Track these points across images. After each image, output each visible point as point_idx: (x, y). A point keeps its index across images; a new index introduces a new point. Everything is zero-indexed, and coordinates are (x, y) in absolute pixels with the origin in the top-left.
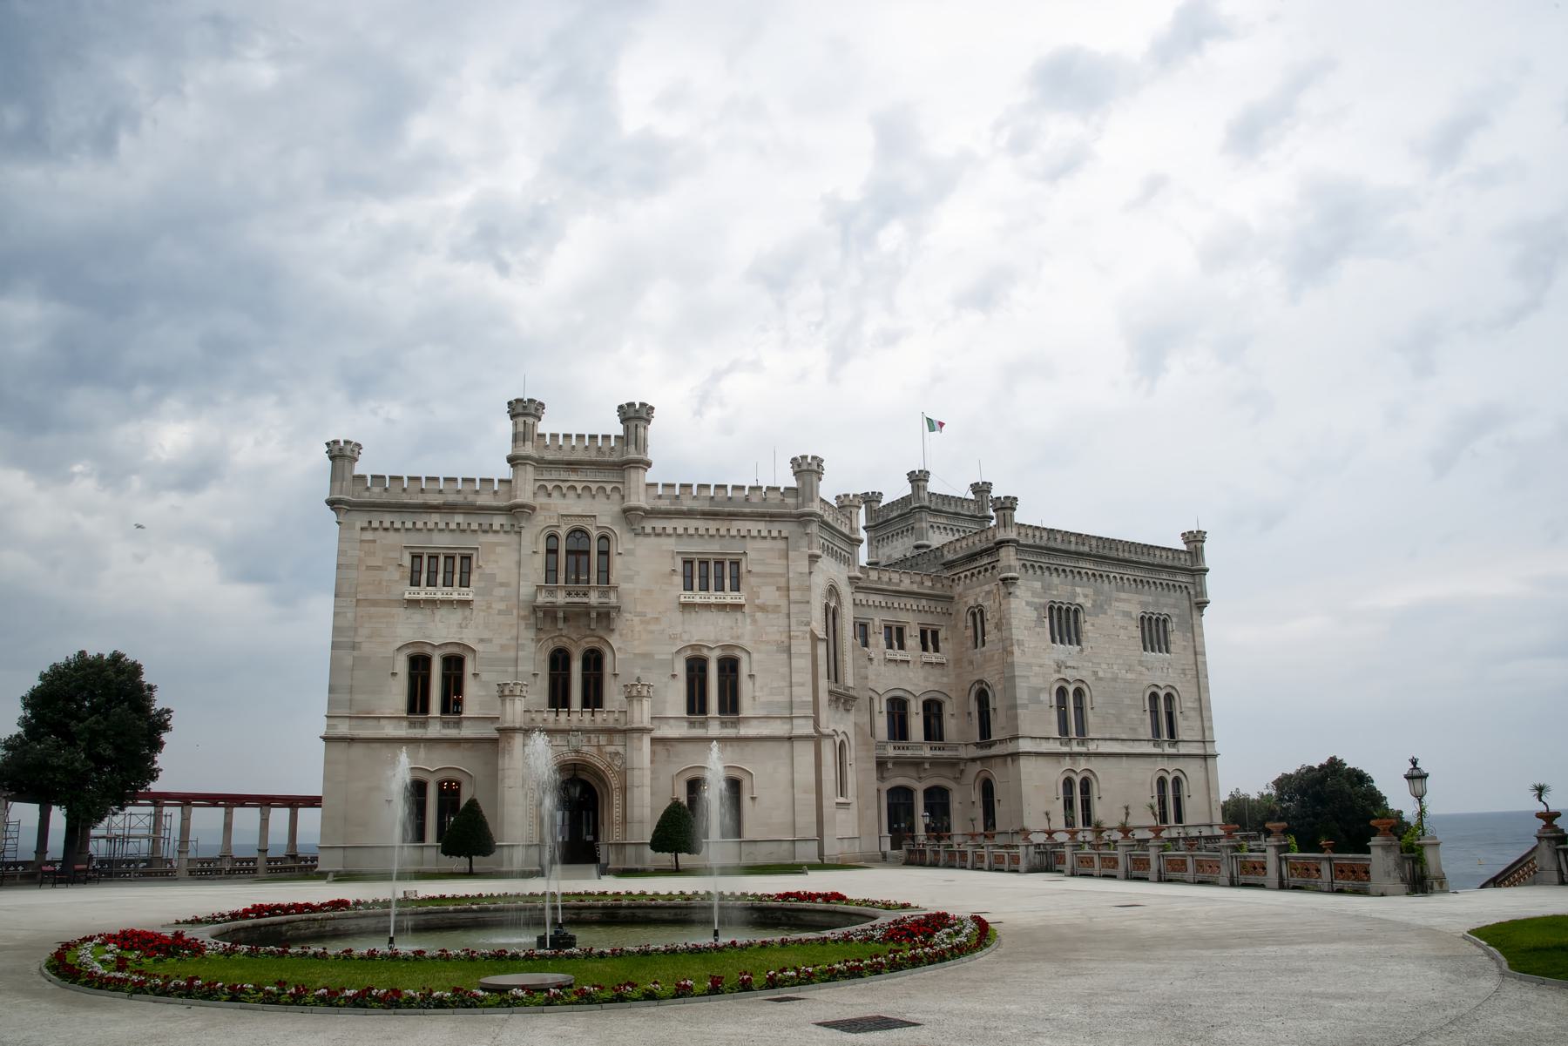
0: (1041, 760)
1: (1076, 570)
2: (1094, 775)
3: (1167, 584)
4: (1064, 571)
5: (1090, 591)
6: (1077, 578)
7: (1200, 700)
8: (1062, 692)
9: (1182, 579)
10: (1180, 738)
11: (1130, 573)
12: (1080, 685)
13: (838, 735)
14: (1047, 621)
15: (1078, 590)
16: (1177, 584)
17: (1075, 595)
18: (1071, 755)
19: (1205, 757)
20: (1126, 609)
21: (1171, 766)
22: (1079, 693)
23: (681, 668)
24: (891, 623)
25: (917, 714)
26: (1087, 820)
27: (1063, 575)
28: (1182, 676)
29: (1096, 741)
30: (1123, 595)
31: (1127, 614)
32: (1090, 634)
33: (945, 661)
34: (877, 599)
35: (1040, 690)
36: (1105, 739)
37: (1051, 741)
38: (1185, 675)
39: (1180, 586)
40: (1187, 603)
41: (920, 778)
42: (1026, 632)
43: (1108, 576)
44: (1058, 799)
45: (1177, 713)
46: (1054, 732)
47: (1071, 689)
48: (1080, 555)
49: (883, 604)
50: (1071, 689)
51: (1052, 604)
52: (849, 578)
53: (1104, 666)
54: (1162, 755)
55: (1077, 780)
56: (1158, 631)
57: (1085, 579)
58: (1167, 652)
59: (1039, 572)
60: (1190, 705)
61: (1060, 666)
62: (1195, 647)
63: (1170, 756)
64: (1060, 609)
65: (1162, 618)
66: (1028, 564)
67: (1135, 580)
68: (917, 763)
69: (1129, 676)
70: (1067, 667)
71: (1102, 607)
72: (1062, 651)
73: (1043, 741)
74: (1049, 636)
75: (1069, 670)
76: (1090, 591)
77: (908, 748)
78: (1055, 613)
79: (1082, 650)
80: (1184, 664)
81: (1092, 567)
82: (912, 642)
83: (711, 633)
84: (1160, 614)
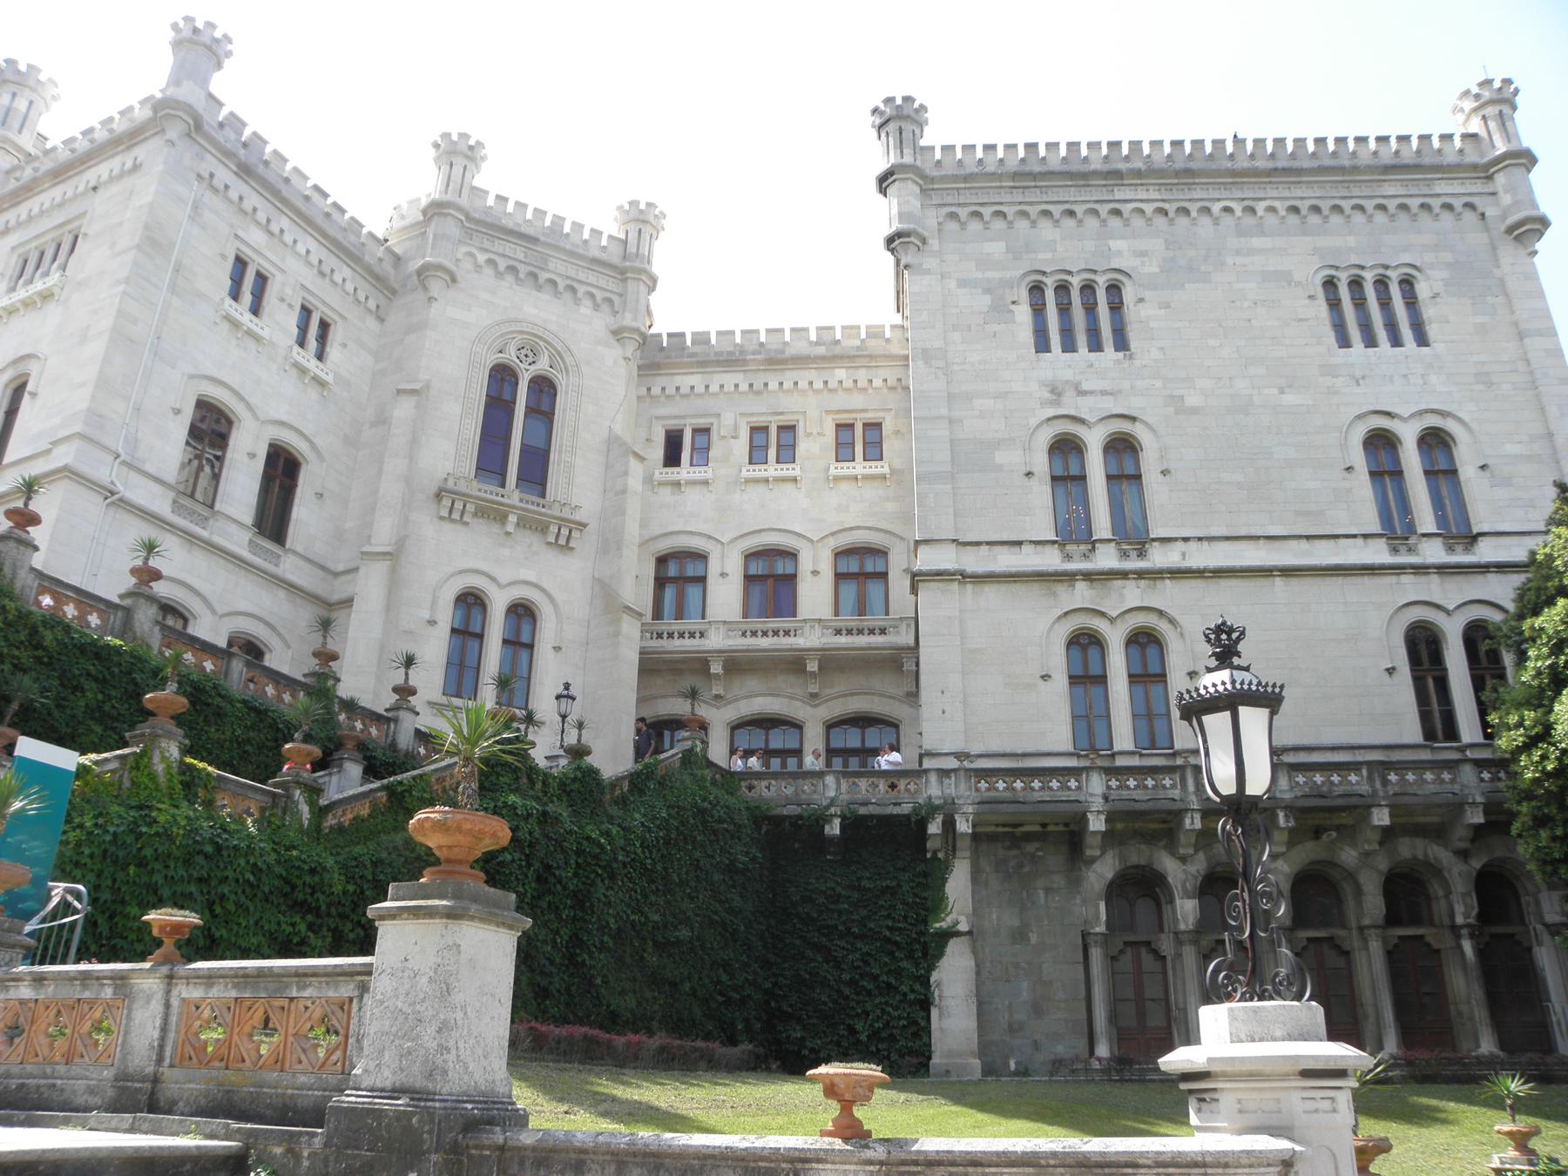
1: (1104, 209)
2: (1172, 621)
3: (1403, 207)
4: (1071, 213)
5: (1155, 245)
6: (1115, 222)
8: (1066, 448)
10: (1486, 529)
11: (1278, 195)
12: (1125, 426)
13: (500, 586)
14: (1024, 313)
15: (1116, 245)
16: (1436, 203)
18: (1088, 576)
20: (1271, 268)
21: (1451, 592)
22: (1122, 447)
24: (770, 418)
25: (815, 573)
27: (1069, 223)
28: (1481, 387)
29: (1180, 544)
30: (1257, 242)
31: (1284, 278)
32: (1152, 324)
33: (886, 470)
34: (730, 379)
36: (1211, 539)
37: (1026, 548)
38: (1490, 384)
39: (1448, 207)
40: (1476, 238)
41: (814, 696)
42: (957, 336)
43: (1206, 210)
44: (1046, 677)
45: (1468, 472)
47: (1094, 441)
48: (1116, 175)
49: (744, 387)
50: (1094, 441)
51: (1039, 277)
52: (615, 333)
54: (1420, 569)
55: (1115, 639)
56: (1385, 303)
57: (1138, 222)
58: (1422, 340)
59: (999, 224)
60: (1511, 449)
61: (1056, 392)
62: (1516, 324)
63: (1443, 569)
64: (1062, 288)
65: (1394, 275)
66: (963, 213)
67: (1295, 210)
68: (794, 664)
69: (1289, 399)
70: (1082, 393)
73: (1005, 549)
74: (1026, 334)
75: (1089, 401)
76: (1155, 245)
77: (765, 634)
78: (1050, 295)
79: (1131, 357)
80: (1484, 363)
81: (1156, 196)
82: (815, 445)
84: (1387, 267)
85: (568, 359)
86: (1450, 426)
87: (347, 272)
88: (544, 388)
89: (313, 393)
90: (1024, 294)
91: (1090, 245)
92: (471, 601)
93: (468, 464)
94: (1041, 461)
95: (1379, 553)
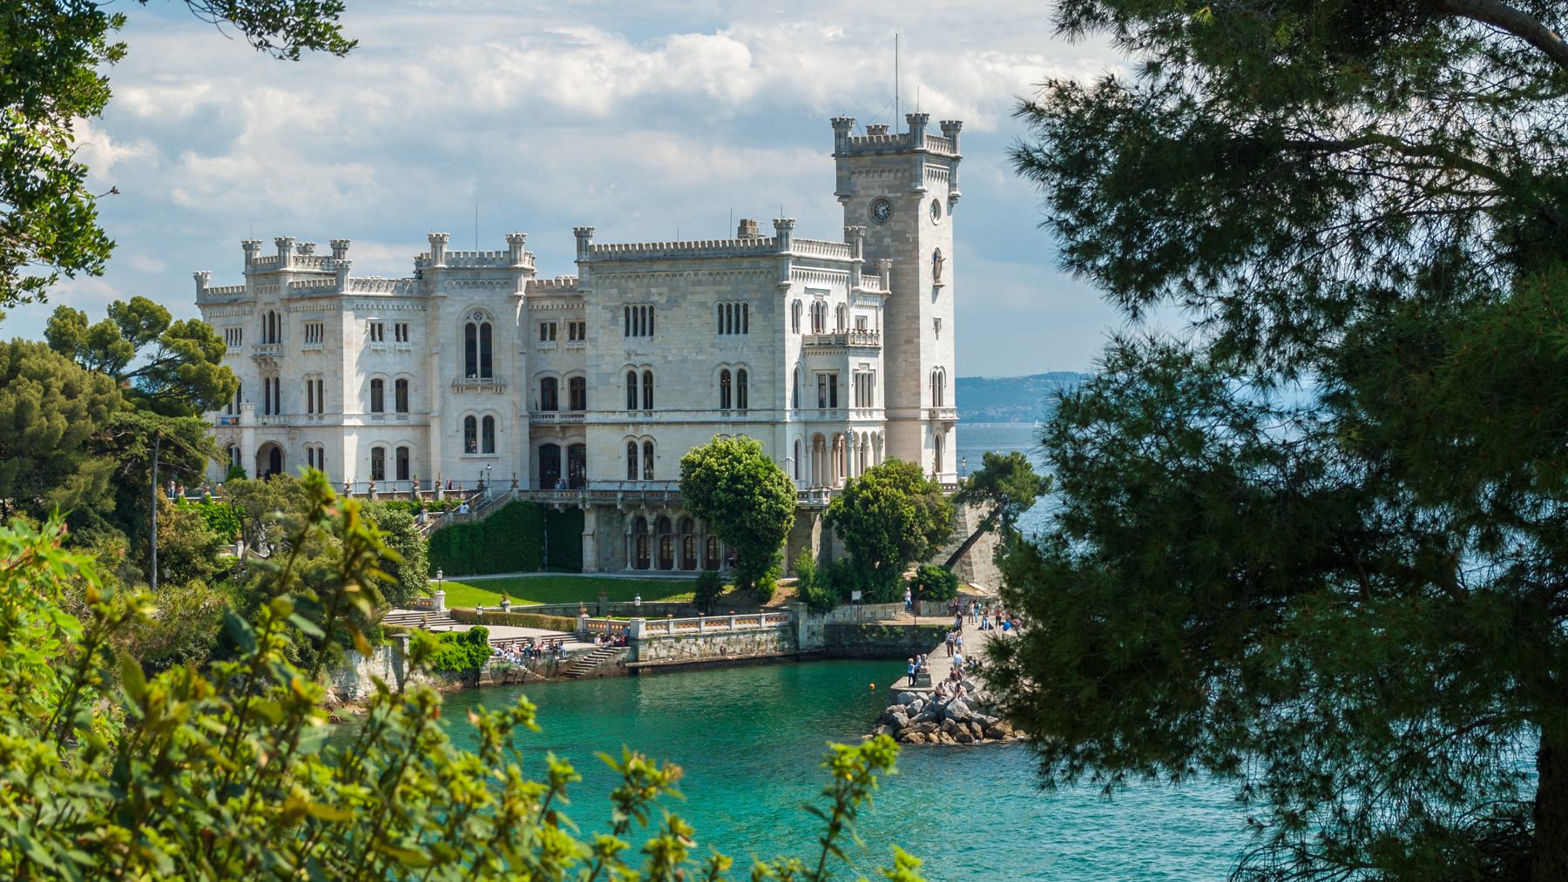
0: (606, 427)
5: (665, 290)
7: (773, 373)
8: (632, 377)
9: (764, 263)
14: (622, 320)
15: (653, 290)
17: (649, 294)
19: (773, 423)
22: (648, 377)
23: (304, 387)
30: (699, 289)
31: (703, 305)
34: (560, 302)
35: (610, 375)
46: (623, 405)
53: (674, 351)
54: (726, 423)
60: (763, 378)
63: (734, 423)
64: (635, 309)
67: (711, 274)
69: (699, 357)
71: (676, 301)
72: (633, 342)
74: (622, 330)
76: (665, 290)
83: (313, 364)
85: (494, 315)
86: (747, 369)
87: (408, 303)
88: (486, 329)
89: (406, 355)
90: (623, 312)
91: (644, 290)
92: (470, 422)
93: (463, 371)
94: (623, 381)
95: (718, 417)
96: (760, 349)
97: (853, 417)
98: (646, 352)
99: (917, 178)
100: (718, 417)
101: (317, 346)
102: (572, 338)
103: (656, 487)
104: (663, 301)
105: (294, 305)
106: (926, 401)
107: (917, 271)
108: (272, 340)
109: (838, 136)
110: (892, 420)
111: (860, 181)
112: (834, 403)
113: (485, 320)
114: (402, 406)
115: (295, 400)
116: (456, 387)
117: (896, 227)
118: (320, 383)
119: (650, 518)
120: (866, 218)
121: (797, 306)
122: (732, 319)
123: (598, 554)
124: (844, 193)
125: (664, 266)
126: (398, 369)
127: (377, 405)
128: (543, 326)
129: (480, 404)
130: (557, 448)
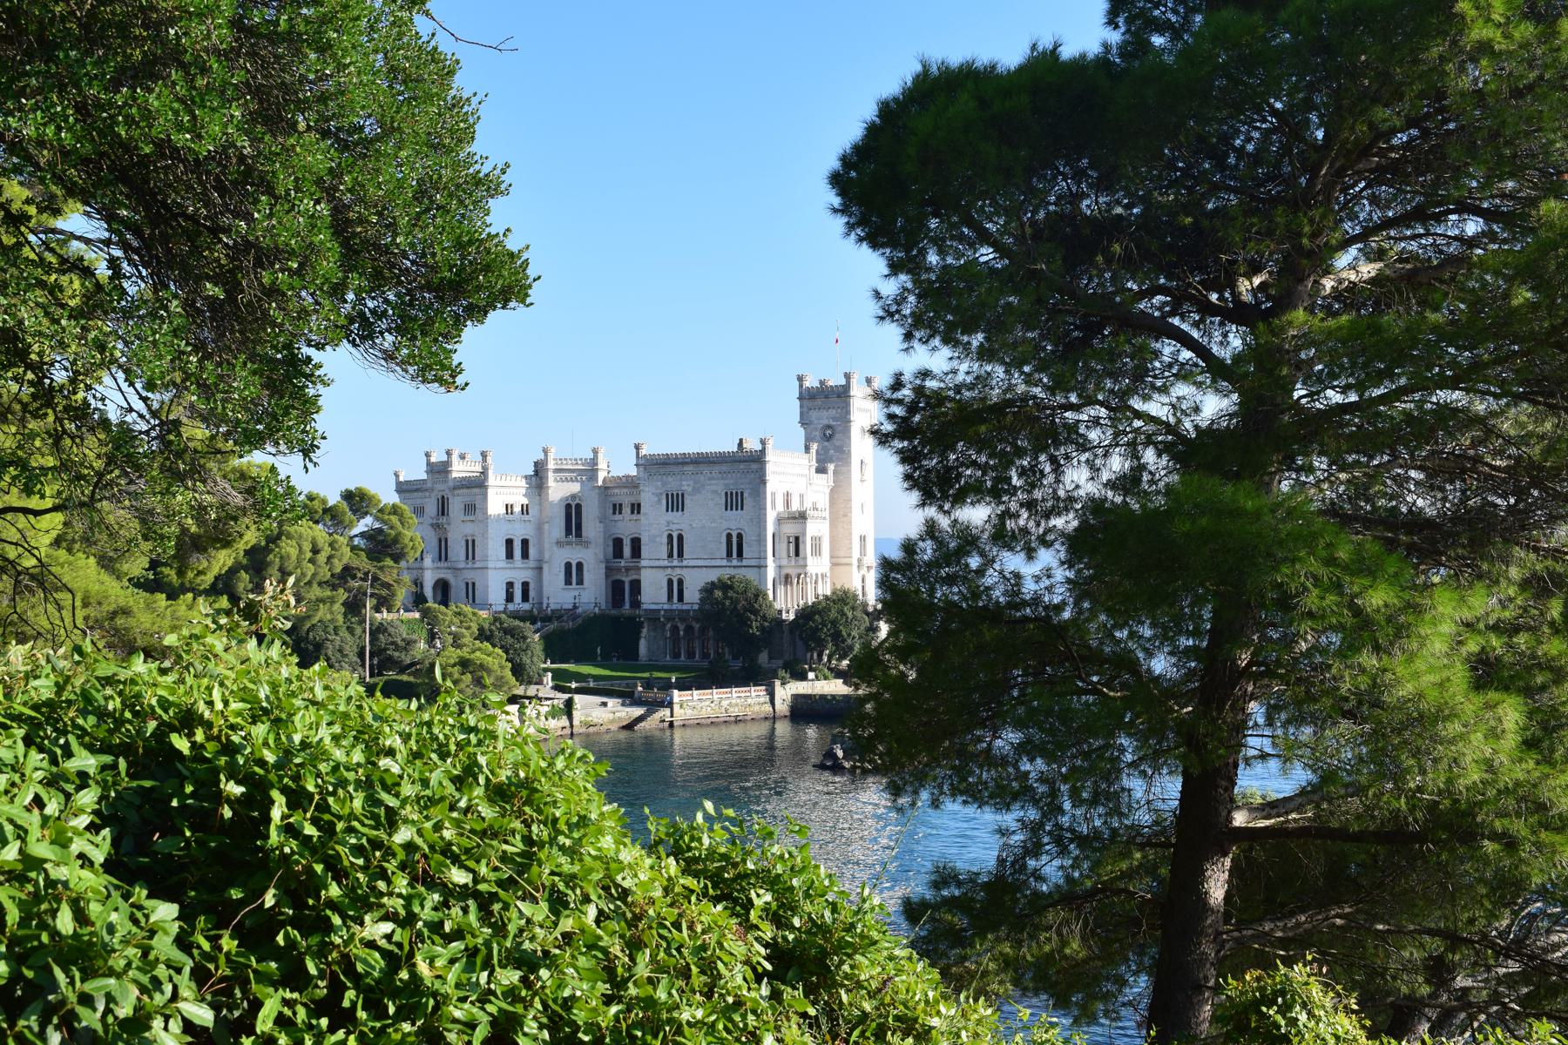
8: (670, 537)
9: (754, 466)
11: (717, 468)
14: (664, 502)
22: (680, 538)
23: (464, 543)
26: (681, 599)
34: (625, 490)
46: (665, 555)
83: (469, 529)
88: (578, 507)
92: (568, 566)
93: (563, 533)
94: (665, 540)
95: (724, 563)
96: (751, 520)
97: (810, 560)
98: (678, 522)
99: (848, 413)
100: (724, 563)
101: (472, 518)
102: (632, 512)
103: (685, 607)
104: (690, 489)
105: (456, 492)
106: (856, 554)
107: (850, 471)
108: (443, 514)
109: (801, 386)
110: (834, 565)
111: (814, 415)
112: (797, 554)
113: (577, 501)
114: (525, 555)
115: (457, 551)
116: (559, 543)
117: (837, 443)
118: (473, 541)
119: (682, 627)
120: (818, 438)
121: (773, 494)
122: (734, 501)
123: (649, 650)
124: (804, 422)
125: (690, 468)
126: (523, 532)
127: (510, 555)
128: (615, 505)
129: (574, 554)
130: (623, 582)
